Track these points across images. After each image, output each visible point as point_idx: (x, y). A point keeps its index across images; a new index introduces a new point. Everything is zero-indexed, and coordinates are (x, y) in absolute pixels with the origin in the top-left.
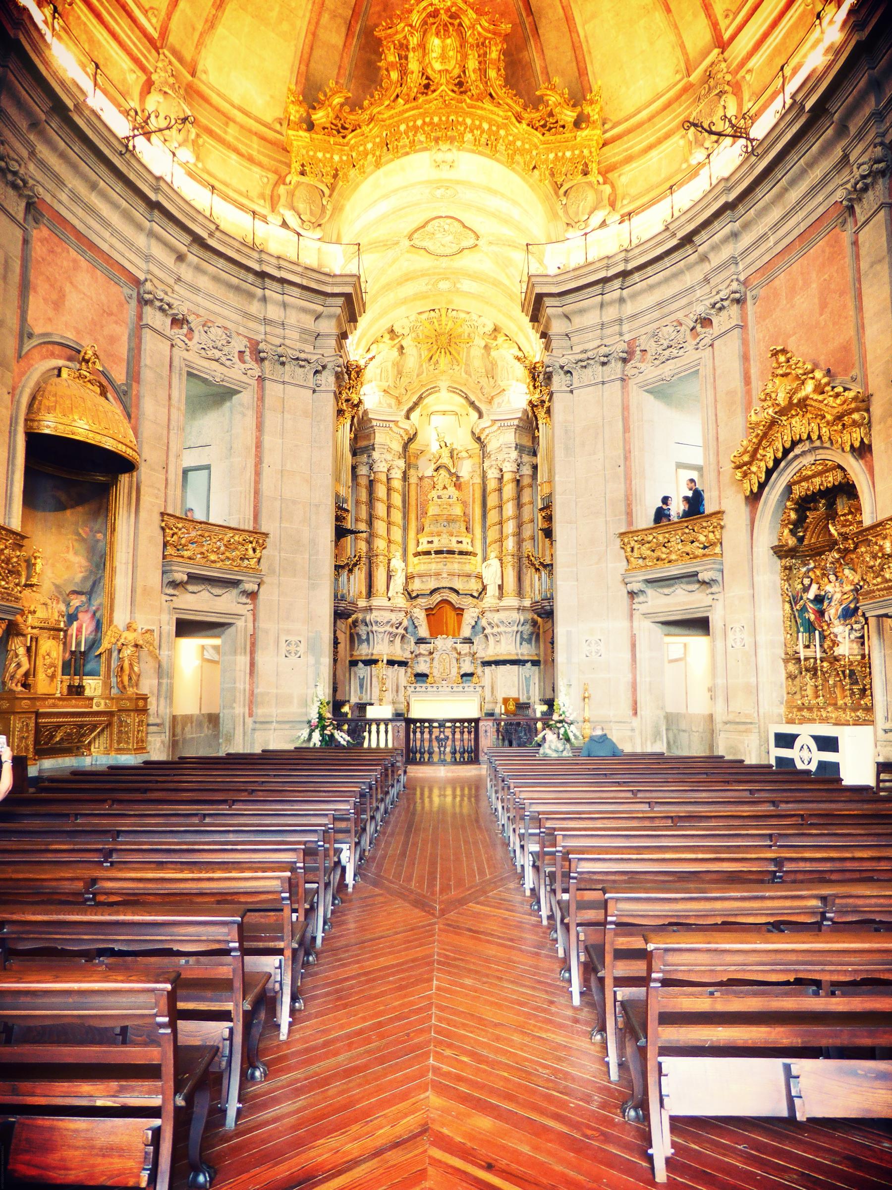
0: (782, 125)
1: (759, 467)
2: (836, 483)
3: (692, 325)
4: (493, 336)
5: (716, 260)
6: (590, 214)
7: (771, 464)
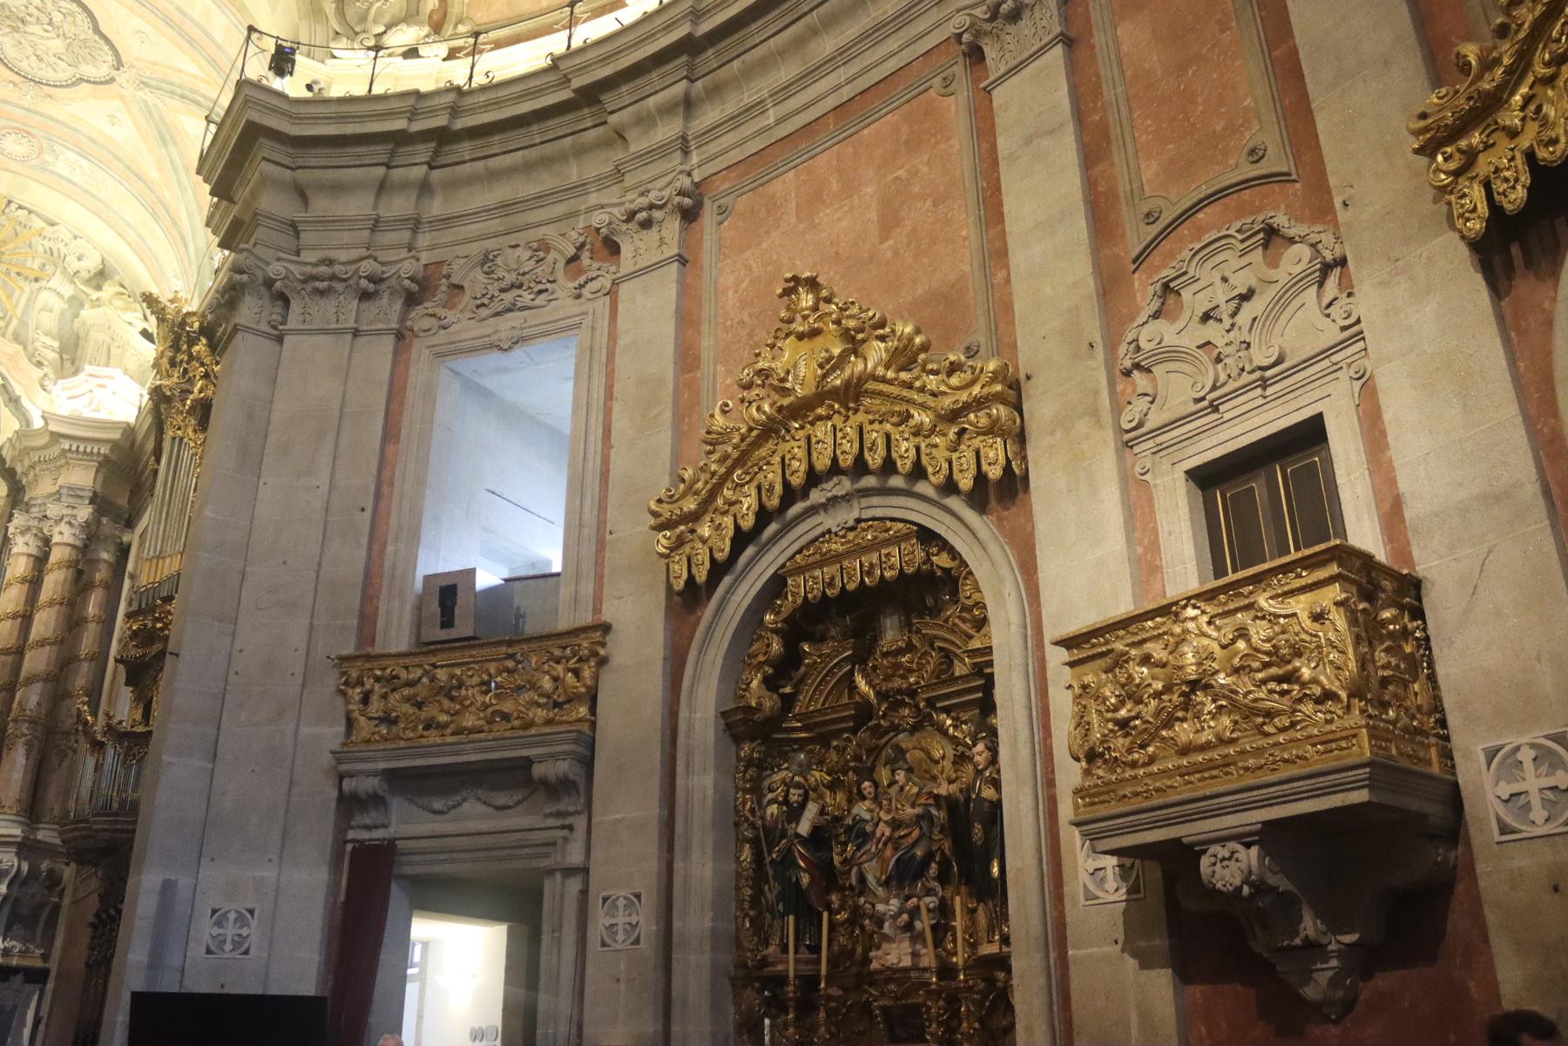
2: (909, 570)
3: (571, 251)
4: (94, 283)
5: (639, 143)
6: (389, 27)
7: (748, 523)
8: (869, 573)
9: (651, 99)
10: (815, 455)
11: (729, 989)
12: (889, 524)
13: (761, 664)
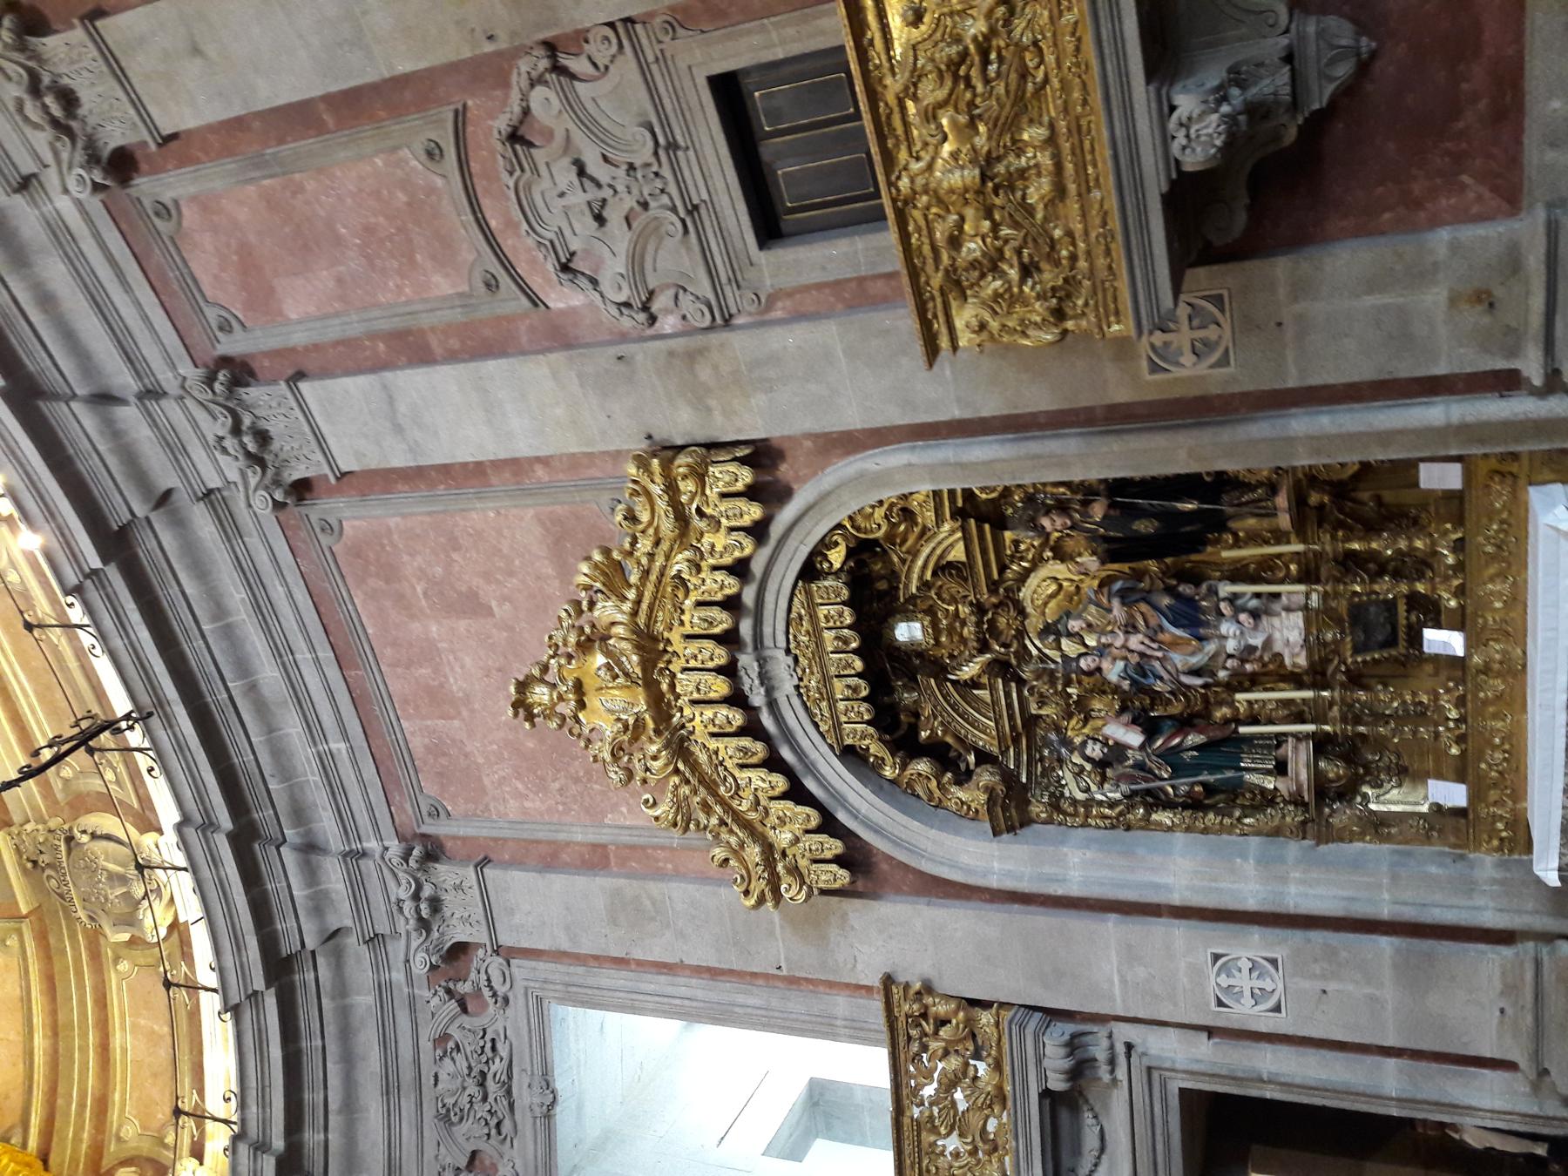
0: (118, 643)
1: (782, 821)
2: (845, 593)
3: (453, 1004)
7: (780, 782)
8: (846, 642)
9: (295, 893)
10: (713, 695)
11: (1332, 846)
12: (794, 615)
13: (940, 786)
